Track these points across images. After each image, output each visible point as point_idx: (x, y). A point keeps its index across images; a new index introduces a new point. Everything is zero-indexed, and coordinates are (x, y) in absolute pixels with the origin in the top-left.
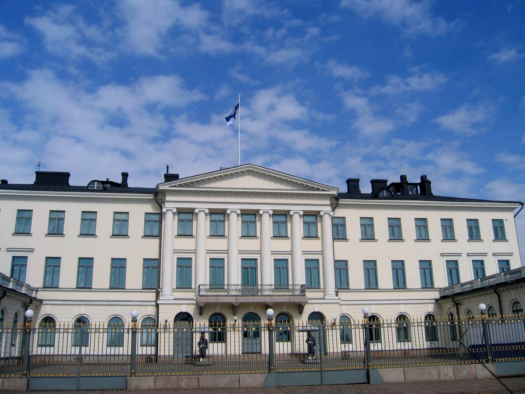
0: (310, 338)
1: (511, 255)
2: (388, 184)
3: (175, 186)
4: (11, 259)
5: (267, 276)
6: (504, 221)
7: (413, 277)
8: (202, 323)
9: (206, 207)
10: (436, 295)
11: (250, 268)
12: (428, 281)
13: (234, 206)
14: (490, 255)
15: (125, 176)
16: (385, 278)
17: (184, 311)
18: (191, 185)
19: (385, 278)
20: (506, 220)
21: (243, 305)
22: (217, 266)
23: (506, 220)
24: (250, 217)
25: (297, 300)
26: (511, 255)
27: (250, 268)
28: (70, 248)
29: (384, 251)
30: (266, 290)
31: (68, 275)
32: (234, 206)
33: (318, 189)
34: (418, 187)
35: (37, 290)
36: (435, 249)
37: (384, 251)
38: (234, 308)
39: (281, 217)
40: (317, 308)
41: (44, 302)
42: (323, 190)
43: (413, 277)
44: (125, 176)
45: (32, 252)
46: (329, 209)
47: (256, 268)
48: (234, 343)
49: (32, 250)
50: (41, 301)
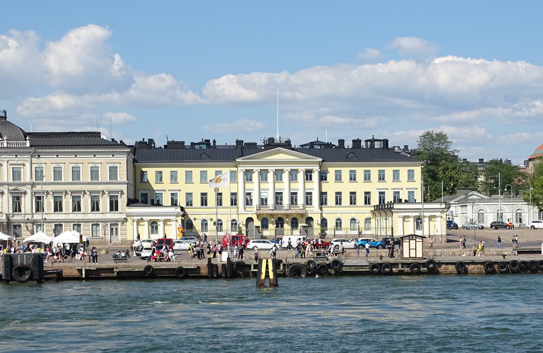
4: (170, 195)
5: (286, 200)
7: (360, 199)
8: (257, 223)
10: (373, 209)
12: (367, 201)
25: (301, 212)
28: (197, 189)
29: (346, 187)
31: (197, 200)
32: (272, 169)
36: (374, 187)
37: (346, 187)
38: (272, 215)
39: (293, 175)
43: (360, 199)
46: (318, 168)
48: (271, 231)
49: (180, 191)
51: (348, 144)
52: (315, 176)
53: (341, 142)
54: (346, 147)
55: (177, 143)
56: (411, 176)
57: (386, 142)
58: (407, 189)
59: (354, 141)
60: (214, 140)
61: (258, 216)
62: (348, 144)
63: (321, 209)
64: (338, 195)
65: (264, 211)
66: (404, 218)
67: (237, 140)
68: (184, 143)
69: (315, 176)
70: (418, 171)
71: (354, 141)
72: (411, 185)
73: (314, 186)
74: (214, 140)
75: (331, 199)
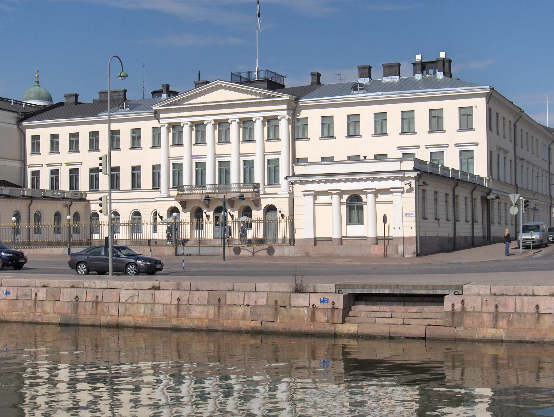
0: (169, 230)
1: (477, 144)
3: (164, 106)
6: (474, 108)
8: (185, 216)
11: (224, 169)
13: (208, 118)
14: (452, 146)
20: (476, 107)
22: (200, 168)
23: (476, 107)
24: (222, 126)
26: (477, 144)
27: (224, 169)
30: (233, 188)
33: (273, 97)
35: (86, 193)
40: (270, 202)
41: (90, 202)
45: (81, 164)
46: (285, 113)
50: (89, 201)
52: (284, 128)
56: (466, 121)
58: (457, 145)
61: (184, 204)
65: (198, 194)
66: (317, 194)
69: (284, 128)
70: (479, 107)
72: (466, 137)
73: (281, 148)
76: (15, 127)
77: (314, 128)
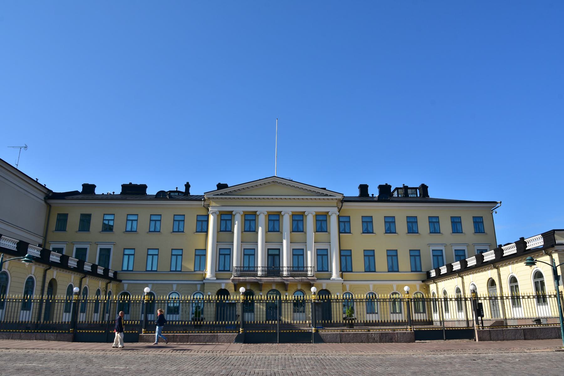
2: (392, 190)
3: (218, 195)
9: (242, 209)
15: (188, 186)
16: (381, 262)
17: (223, 288)
18: (230, 193)
19: (381, 262)
21: (270, 283)
34: (418, 190)
42: (330, 196)
44: (188, 186)
46: (336, 210)
47: (279, 255)
51: (374, 191)
53: (364, 189)
54: (370, 195)
55: (136, 186)
57: (424, 188)
59: (381, 187)
60: (188, 183)
62: (374, 191)
63: (342, 276)
64: (370, 255)
67: (219, 184)
68: (144, 187)
71: (381, 187)
74: (188, 183)
75: (358, 262)
76: (43, 202)
77: (356, 225)
